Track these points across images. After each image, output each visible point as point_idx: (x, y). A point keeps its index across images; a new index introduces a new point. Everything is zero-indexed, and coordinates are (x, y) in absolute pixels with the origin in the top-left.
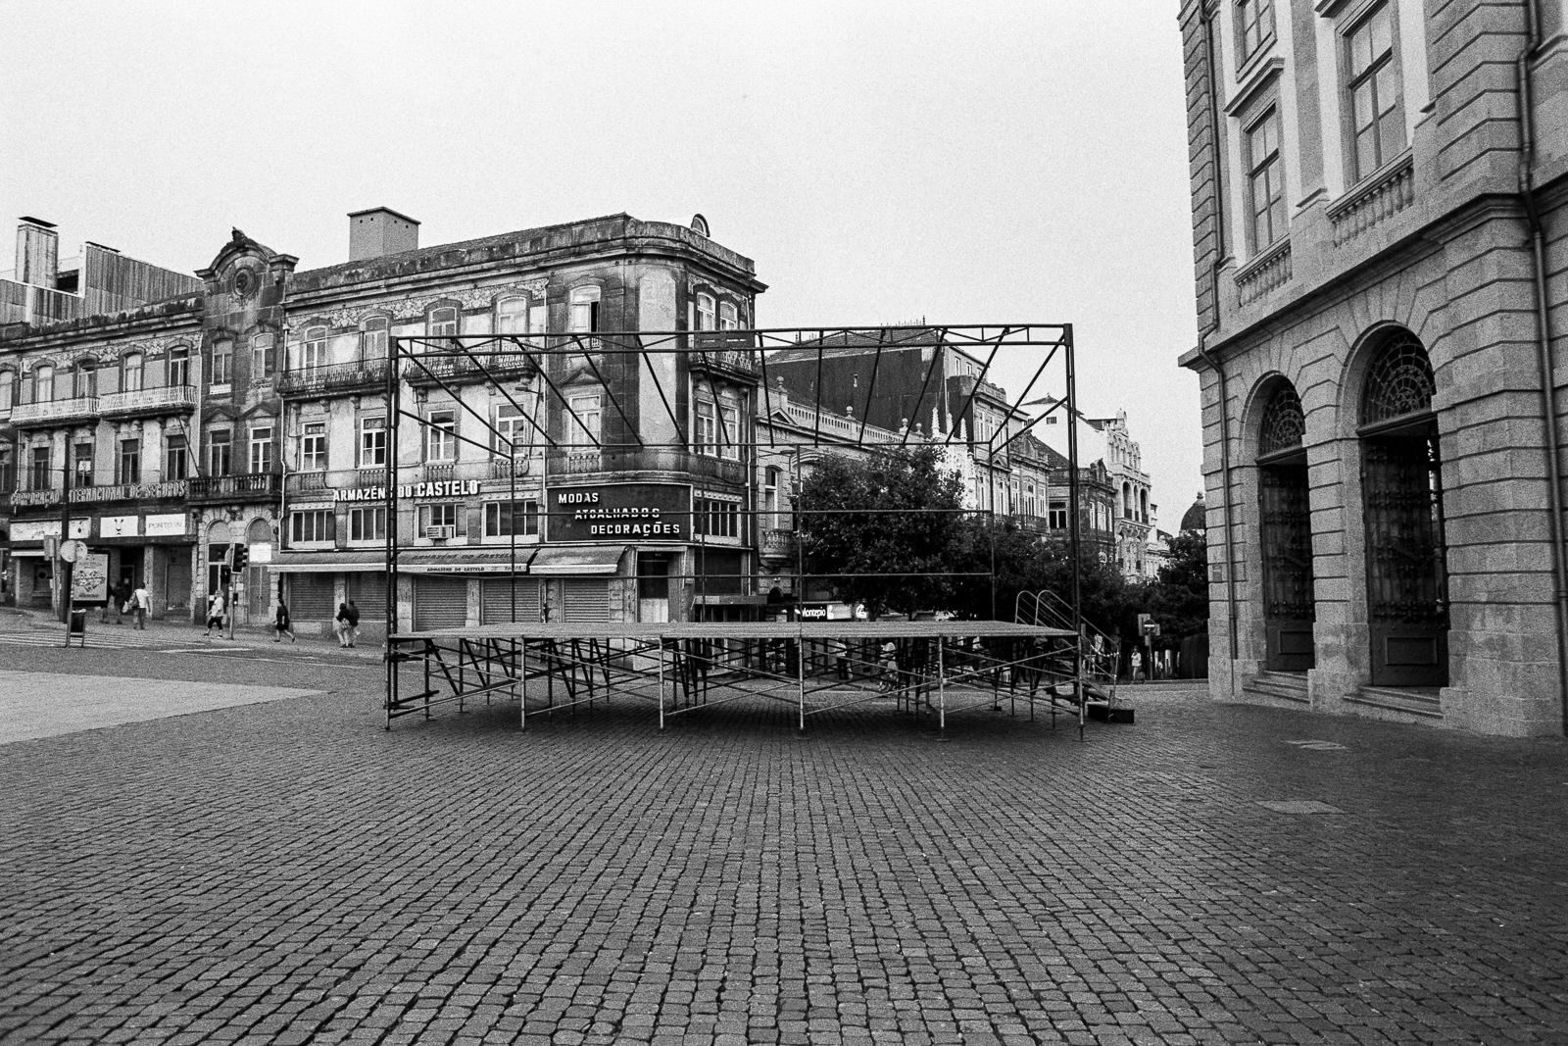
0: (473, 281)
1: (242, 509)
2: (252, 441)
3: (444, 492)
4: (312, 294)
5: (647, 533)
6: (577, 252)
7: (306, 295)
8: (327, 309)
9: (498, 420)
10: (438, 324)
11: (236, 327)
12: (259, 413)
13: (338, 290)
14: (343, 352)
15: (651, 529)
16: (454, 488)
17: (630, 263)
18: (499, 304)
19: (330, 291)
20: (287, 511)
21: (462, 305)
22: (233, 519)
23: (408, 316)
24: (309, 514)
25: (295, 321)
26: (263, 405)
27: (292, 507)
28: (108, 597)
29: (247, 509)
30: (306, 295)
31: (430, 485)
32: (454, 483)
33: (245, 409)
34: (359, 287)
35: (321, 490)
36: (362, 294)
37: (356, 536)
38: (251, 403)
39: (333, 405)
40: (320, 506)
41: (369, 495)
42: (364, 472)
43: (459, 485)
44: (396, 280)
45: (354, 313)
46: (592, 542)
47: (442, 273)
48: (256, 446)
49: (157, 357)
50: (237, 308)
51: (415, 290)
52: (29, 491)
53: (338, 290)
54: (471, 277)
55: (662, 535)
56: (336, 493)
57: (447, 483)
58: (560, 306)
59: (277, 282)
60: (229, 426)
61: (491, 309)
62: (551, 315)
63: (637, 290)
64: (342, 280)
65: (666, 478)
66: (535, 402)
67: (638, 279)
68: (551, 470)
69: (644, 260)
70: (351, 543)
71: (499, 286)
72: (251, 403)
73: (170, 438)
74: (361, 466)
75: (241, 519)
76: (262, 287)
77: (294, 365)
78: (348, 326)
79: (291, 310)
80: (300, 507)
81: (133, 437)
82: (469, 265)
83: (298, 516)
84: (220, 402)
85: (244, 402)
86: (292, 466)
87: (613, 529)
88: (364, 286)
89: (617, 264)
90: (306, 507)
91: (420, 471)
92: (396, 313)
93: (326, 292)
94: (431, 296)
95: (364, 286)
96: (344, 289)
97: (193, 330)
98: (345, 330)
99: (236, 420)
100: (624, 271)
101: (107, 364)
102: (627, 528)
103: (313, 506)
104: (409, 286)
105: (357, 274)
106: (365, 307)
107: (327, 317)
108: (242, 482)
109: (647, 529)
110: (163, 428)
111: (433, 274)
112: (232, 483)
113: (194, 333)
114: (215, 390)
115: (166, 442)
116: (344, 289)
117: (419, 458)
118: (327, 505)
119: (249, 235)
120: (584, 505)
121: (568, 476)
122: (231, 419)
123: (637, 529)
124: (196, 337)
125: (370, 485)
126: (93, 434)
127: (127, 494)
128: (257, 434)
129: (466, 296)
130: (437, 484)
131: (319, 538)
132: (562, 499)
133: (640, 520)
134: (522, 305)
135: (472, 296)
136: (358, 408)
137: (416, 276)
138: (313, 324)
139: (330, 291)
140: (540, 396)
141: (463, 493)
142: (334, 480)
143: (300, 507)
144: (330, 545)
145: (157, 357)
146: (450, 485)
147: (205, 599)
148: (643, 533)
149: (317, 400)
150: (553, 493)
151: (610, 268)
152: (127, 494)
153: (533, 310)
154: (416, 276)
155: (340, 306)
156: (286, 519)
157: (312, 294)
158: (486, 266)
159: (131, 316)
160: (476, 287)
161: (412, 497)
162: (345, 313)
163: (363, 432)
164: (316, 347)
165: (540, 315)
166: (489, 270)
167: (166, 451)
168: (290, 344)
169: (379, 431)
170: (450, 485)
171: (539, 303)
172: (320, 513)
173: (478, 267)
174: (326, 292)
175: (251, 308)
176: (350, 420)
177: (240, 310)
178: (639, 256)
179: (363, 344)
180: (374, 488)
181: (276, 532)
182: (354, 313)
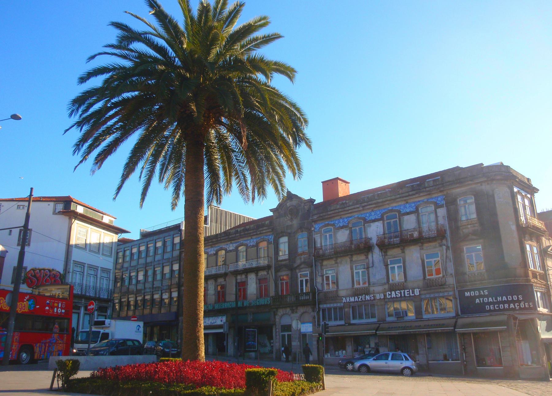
0: (405, 200)
1: (297, 308)
2: (299, 279)
3: (401, 295)
4: (324, 214)
5: (517, 307)
7: (321, 215)
8: (332, 219)
9: (426, 260)
10: (389, 221)
11: (289, 231)
12: (302, 266)
13: (337, 211)
14: (342, 237)
15: (519, 305)
16: (406, 293)
17: (488, 184)
18: (420, 209)
19: (333, 212)
20: (319, 308)
21: (401, 212)
22: (293, 313)
23: (373, 219)
24: (329, 309)
25: (316, 226)
27: (321, 306)
28: (544, 266)
29: (299, 308)
30: (321, 215)
31: (393, 293)
32: (406, 291)
33: (295, 265)
34: (347, 208)
36: (350, 211)
37: (354, 318)
38: (298, 262)
39: (339, 260)
40: (335, 305)
41: (362, 299)
42: (357, 289)
43: (409, 291)
44: (366, 204)
45: (346, 220)
46: (487, 314)
47: (389, 198)
48: (302, 281)
50: (289, 223)
51: (376, 207)
53: (337, 211)
54: (405, 199)
55: (525, 308)
56: (344, 299)
57: (402, 291)
59: (308, 211)
60: (289, 272)
61: (416, 211)
62: (448, 211)
64: (338, 207)
66: (445, 251)
68: (458, 282)
69: (494, 182)
70: (353, 322)
71: (419, 201)
72: (298, 262)
73: (260, 280)
74: (356, 286)
75: (296, 312)
76: (300, 214)
77: (318, 245)
78: (343, 226)
79: (315, 221)
80: (325, 306)
82: (402, 194)
83: (324, 310)
84: (284, 263)
85: (295, 262)
86: (320, 288)
87: (499, 307)
88: (350, 208)
89: (481, 185)
90: (328, 306)
91: (386, 287)
92: (367, 218)
93: (331, 212)
94: (384, 209)
95: (350, 208)
96: (340, 210)
97: (269, 234)
98: (342, 228)
102: (506, 306)
103: (332, 305)
104: (374, 206)
105: (346, 203)
106: (351, 217)
107: (332, 223)
108: (297, 296)
109: (518, 306)
110: (257, 275)
111: (384, 200)
112: (293, 298)
113: (269, 235)
114: (280, 258)
115: (258, 282)
116: (340, 210)
117: (385, 281)
118: (339, 305)
119: (293, 192)
120: (480, 296)
121: (468, 284)
123: (512, 306)
124: (270, 237)
125: (362, 295)
126: (225, 280)
127: (243, 304)
128: (302, 276)
129: (402, 207)
130: (397, 292)
131: (336, 319)
132: (467, 294)
133: (513, 302)
134: (432, 208)
135: (405, 207)
136: (351, 261)
137: (375, 201)
138: (326, 226)
139: (333, 212)
140: (448, 248)
141: (411, 295)
142: (342, 293)
143: (325, 306)
144: (342, 322)
145: (253, 246)
146: (404, 292)
147: (280, 349)
148: (515, 307)
149: (332, 258)
150: (461, 293)
152: (243, 304)
153: (439, 210)
154: (375, 201)
155: (338, 218)
156: (319, 311)
157: (324, 214)
158: (410, 193)
159: (240, 231)
160: (407, 203)
161: (384, 298)
162: (341, 221)
164: (328, 237)
165: (442, 212)
166: (414, 195)
168: (315, 236)
169: (363, 270)
170: (404, 292)
171: (442, 206)
172: (335, 308)
173: (407, 194)
174: (331, 212)
175: (296, 223)
176: (348, 266)
177: (291, 223)
179: (351, 232)
180: (364, 295)
181: (314, 318)
182: (346, 220)
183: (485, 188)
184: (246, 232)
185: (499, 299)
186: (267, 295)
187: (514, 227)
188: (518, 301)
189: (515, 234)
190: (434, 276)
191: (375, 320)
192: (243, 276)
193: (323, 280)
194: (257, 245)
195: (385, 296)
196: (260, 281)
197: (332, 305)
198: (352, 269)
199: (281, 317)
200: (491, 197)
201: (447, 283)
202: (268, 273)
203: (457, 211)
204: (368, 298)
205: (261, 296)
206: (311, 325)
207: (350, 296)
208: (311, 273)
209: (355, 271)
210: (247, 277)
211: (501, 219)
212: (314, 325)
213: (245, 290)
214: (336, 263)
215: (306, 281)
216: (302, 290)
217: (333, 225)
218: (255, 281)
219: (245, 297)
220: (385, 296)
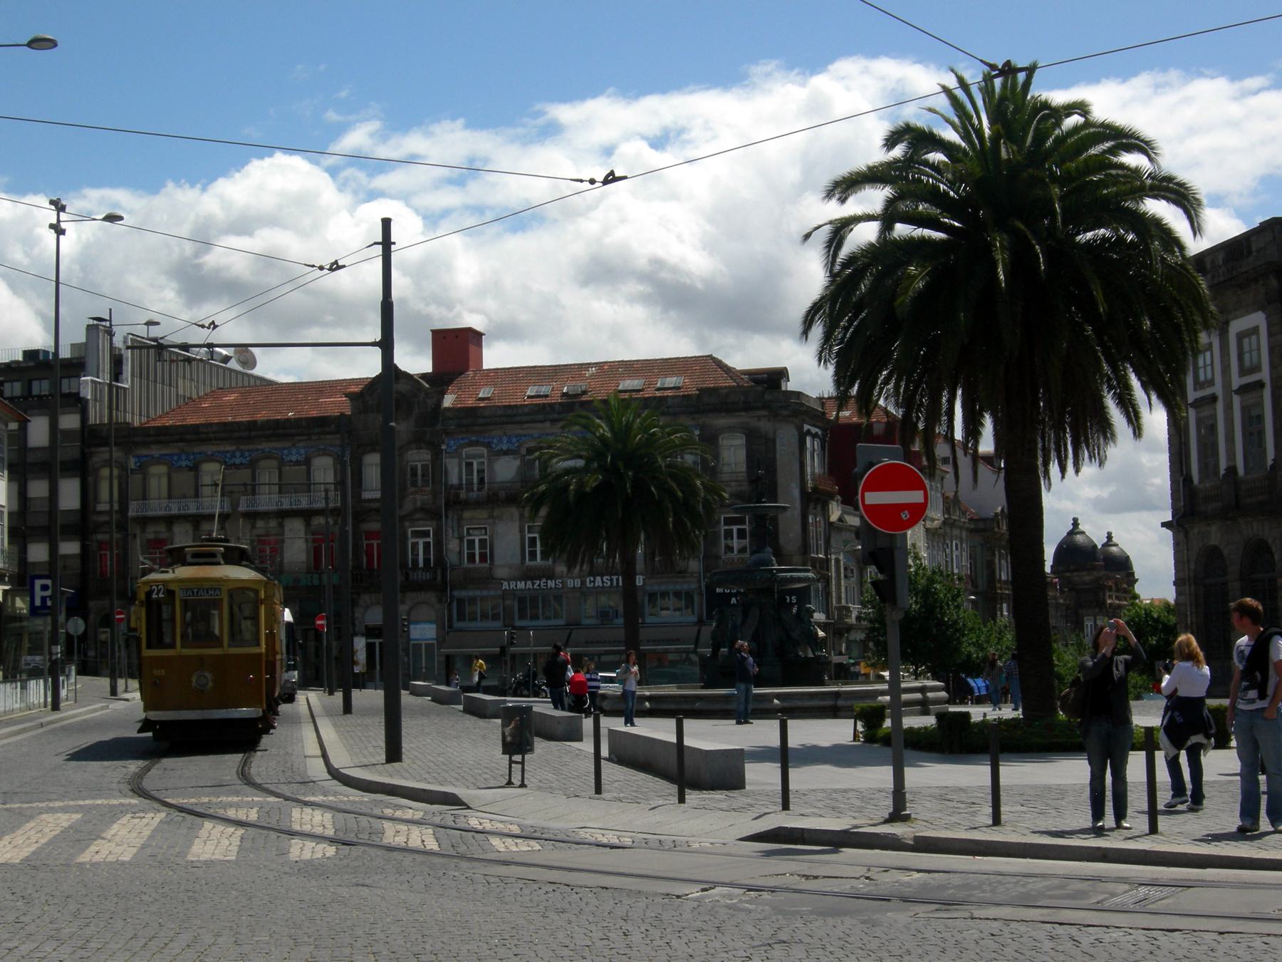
2: (411, 541)
12: (418, 516)
20: (452, 597)
26: (422, 509)
27: (456, 593)
35: (487, 579)
37: (522, 617)
48: (415, 545)
49: (298, 463)
57: (615, 578)
67: (775, 432)
83: (461, 602)
90: (471, 593)
98: (506, 453)
103: (478, 593)
110: (308, 524)
142: (500, 572)
145: (298, 463)
162: (505, 439)
163: (528, 535)
184: (280, 431)
187: (796, 493)
189: (798, 504)
191: (561, 622)
192: (273, 523)
193: (461, 546)
194: (307, 462)
195: (583, 583)
197: (478, 593)
198: (522, 531)
199: (367, 608)
200: (771, 442)
201: (689, 570)
204: (551, 584)
206: (434, 626)
207: (516, 579)
208: (438, 533)
209: (528, 535)
212: (440, 628)
214: (491, 516)
215: (427, 545)
216: (415, 561)
217: (488, 445)
218: (302, 534)
220: (583, 583)
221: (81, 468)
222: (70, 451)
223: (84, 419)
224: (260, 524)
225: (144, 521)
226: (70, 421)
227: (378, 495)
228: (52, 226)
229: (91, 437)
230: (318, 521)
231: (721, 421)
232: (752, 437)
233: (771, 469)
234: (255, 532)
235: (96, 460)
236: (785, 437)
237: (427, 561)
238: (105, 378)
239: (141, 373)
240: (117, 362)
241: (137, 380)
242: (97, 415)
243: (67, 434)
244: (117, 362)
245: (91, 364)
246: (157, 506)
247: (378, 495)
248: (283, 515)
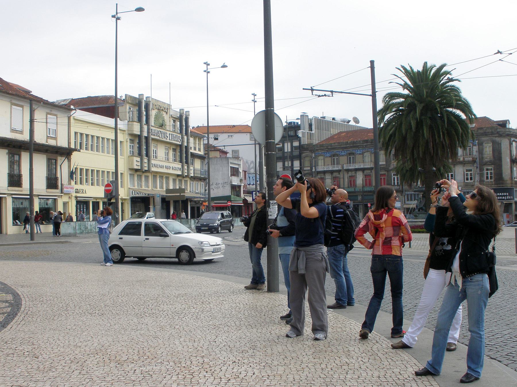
6: (485, 134)
9: (466, 173)
27: (406, 193)
33: (390, 168)
48: (394, 178)
49: (360, 154)
52: (348, 187)
55: (509, 199)
58: (481, 147)
63: (501, 144)
65: (509, 186)
73: (365, 175)
80: (409, 193)
81: (353, 175)
83: (408, 195)
99: (388, 171)
100: (498, 139)
101: (343, 156)
102: (501, 198)
110: (363, 173)
122: (386, 171)
123: (503, 198)
133: (504, 196)
140: (477, 167)
143: (409, 193)
151: (494, 139)
167: (364, 179)
171: (475, 145)
178: (501, 136)
183: (498, 139)
184: (355, 145)
185: (498, 194)
186: (370, 184)
187: (509, 160)
188: (506, 196)
190: (469, 181)
192: (353, 172)
196: (367, 176)
200: (499, 144)
202: (371, 172)
203: (483, 150)
205: (366, 185)
210: (356, 173)
211: (503, 156)
213: (355, 181)
216: (394, 183)
219: (355, 185)
221: (299, 157)
222: (296, 153)
223: (300, 143)
224: (350, 173)
225: (319, 173)
226: (296, 144)
227: (384, 163)
228: (205, 71)
229: (301, 148)
230: (365, 172)
231: (484, 139)
232: (494, 142)
233: (500, 153)
234: (349, 175)
235: (303, 155)
236: (505, 143)
237: (398, 183)
238: (307, 130)
239: (318, 128)
240: (310, 125)
241: (317, 130)
242: (305, 141)
243: (296, 148)
244: (310, 125)
245: (302, 127)
246: (320, 168)
247: (384, 163)
248: (324, 172)
